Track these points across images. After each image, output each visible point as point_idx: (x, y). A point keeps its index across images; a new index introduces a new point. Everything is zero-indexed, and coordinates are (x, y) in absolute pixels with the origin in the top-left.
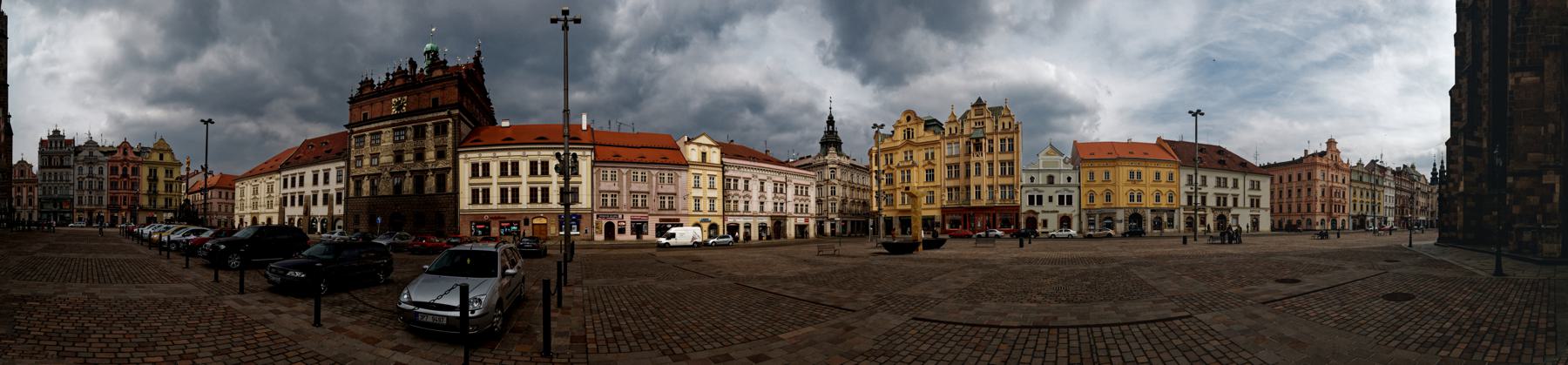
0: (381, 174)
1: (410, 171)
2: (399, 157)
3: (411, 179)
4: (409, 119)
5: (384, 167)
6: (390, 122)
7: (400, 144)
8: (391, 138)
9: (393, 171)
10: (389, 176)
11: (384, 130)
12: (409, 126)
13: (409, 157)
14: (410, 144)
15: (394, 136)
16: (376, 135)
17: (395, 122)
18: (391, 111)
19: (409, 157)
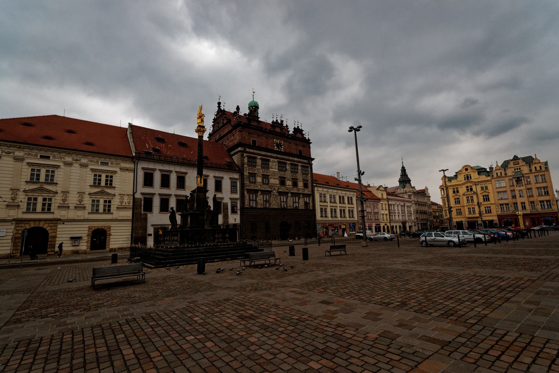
0: (271, 191)
1: (291, 193)
2: (283, 182)
5: (272, 186)
6: (275, 155)
7: (283, 173)
8: (277, 167)
9: (279, 191)
11: (272, 159)
13: (289, 183)
14: (288, 174)
15: (279, 166)
16: (266, 163)
17: (279, 156)
18: (274, 147)
19: (289, 183)
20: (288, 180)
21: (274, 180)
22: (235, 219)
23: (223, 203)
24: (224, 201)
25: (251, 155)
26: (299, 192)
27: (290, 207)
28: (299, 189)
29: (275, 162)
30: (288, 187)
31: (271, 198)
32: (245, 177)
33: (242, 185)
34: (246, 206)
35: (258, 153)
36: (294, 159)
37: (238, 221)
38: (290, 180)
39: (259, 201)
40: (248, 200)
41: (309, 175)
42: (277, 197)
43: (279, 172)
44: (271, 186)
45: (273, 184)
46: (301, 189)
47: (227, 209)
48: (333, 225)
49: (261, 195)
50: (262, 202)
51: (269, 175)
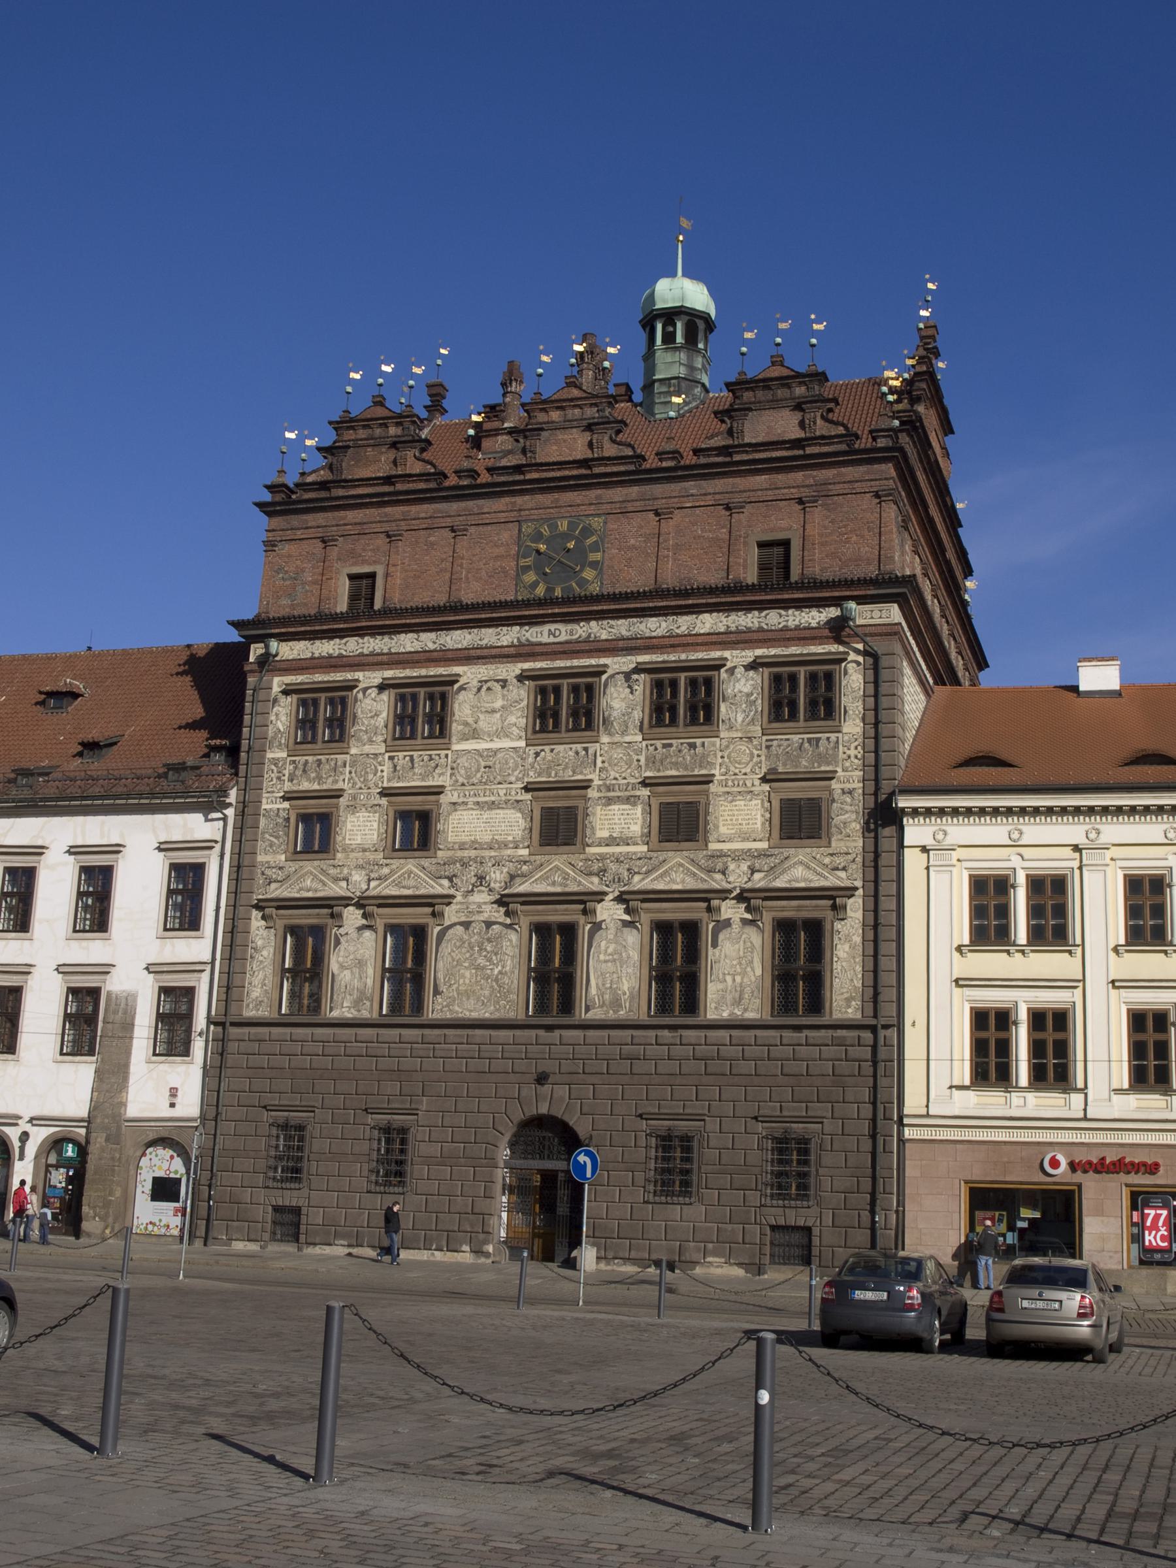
0: (448, 899)
3: (632, 938)
4: (622, 628)
6: (508, 636)
8: (518, 719)
9: (522, 889)
10: (499, 914)
11: (469, 674)
12: (617, 664)
17: (541, 634)
20: (610, 801)
21: (487, 815)
22: (173, 1092)
23: (109, 994)
24: (114, 985)
25: (319, 677)
26: (717, 882)
27: (616, 1003)
28: (722, 855)
29: (504, 683)
30: (602, 858)
31: (446, 948)
32: (263, 822)
33: (241, 871)
34: (249, 1013)
35: (372, 654)
36: (684, 624)
37: (190, 1105)
38: (630, 800)
39: (345, 977)
40: (269, 970)
41: (853, 726)
42: (500, 937)
43: (532, 751)
44: (451, 862)
45: (475, 845)
46: (737, 856)
47: (128, 1026)
48: (1153, 1169)
49: (368, 934)
50: (370, 982)
51: (438, 791)
